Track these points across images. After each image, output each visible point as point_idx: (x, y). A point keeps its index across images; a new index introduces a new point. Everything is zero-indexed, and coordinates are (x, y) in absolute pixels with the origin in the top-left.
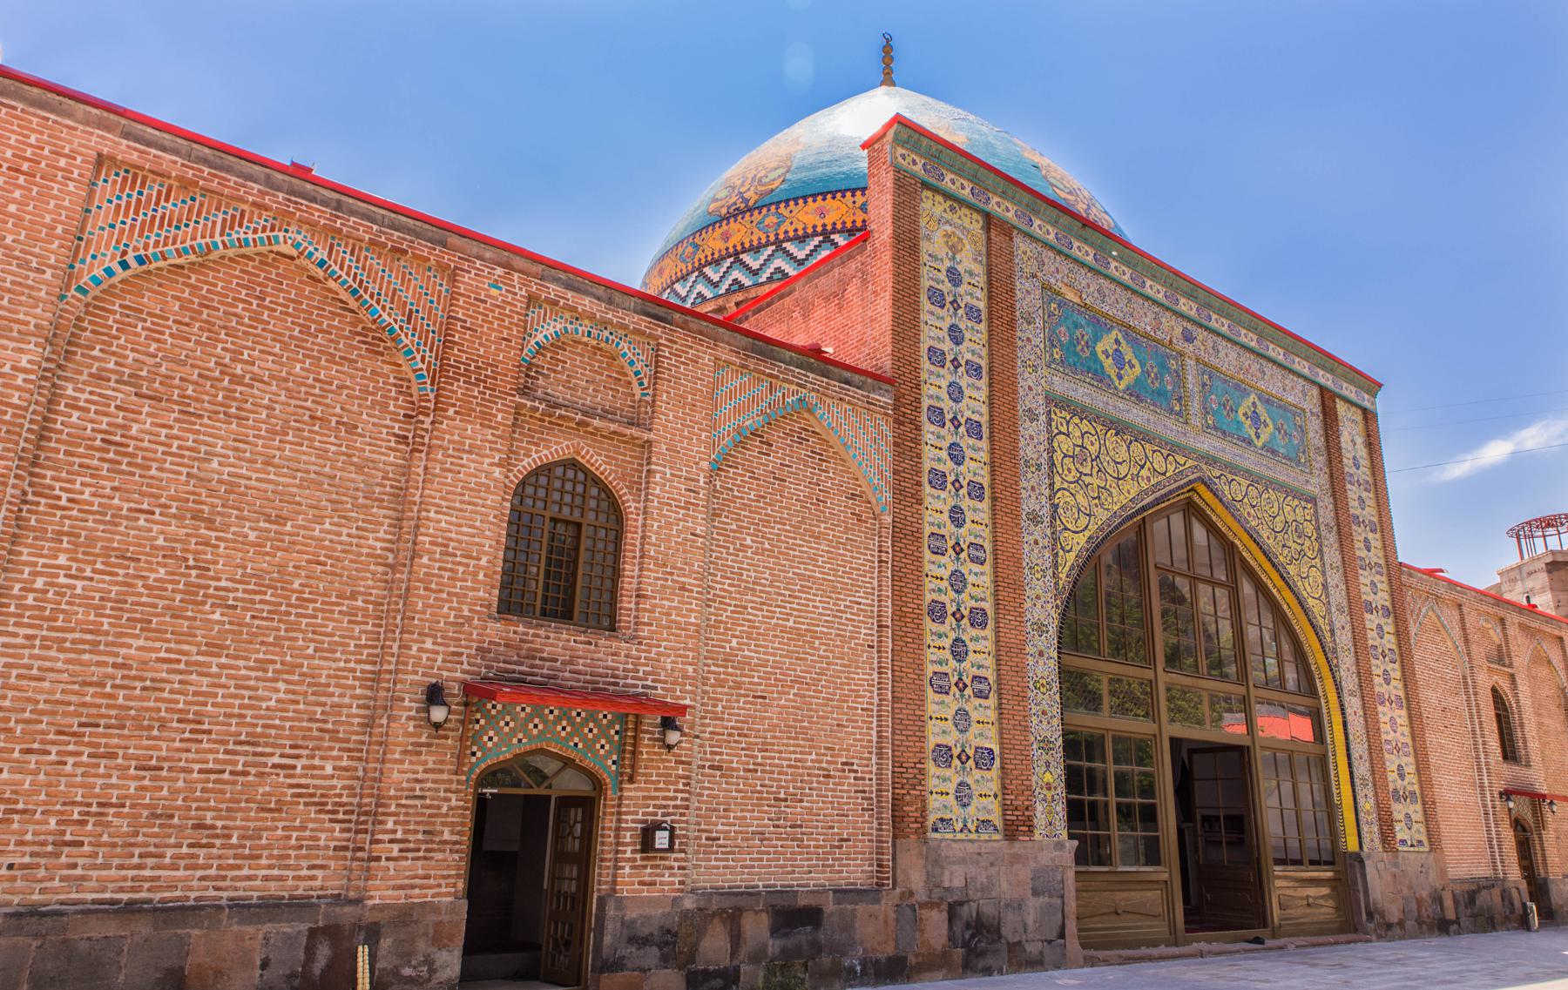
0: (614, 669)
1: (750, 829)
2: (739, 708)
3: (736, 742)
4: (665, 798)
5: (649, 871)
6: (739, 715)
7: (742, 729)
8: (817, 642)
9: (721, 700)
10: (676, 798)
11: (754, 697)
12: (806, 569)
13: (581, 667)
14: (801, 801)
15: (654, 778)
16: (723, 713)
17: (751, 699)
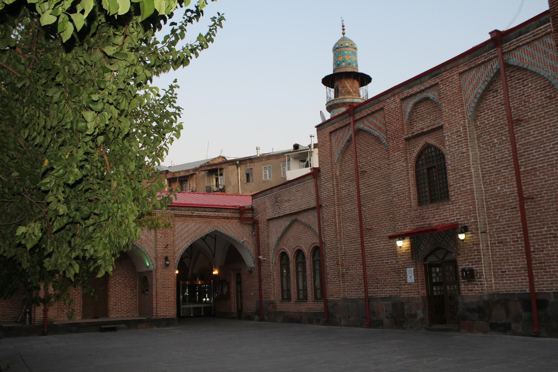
0: (446, 216)
1: (519, 266)
2: (506, 215)
3: (507, 230)
4: (471, 259)
5: (470, 286)
6: (506, 218)
7: (509, 224)
8: (538, 173)
9: (497, 214)
10: (475, 258)
11: (512, 209)
12: (525, 140)
13: (437, 218)
14: (542, 251)
15: (466, 252)
16: (499, 219)
17: (510, 210)
